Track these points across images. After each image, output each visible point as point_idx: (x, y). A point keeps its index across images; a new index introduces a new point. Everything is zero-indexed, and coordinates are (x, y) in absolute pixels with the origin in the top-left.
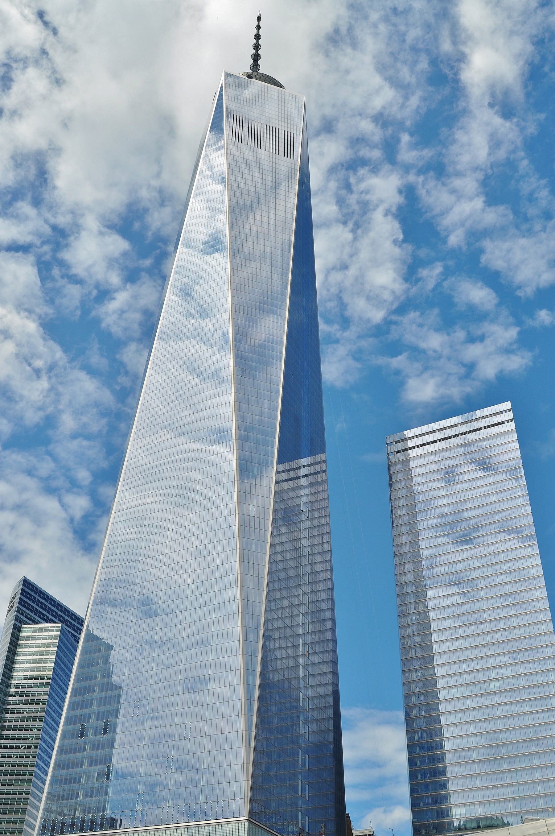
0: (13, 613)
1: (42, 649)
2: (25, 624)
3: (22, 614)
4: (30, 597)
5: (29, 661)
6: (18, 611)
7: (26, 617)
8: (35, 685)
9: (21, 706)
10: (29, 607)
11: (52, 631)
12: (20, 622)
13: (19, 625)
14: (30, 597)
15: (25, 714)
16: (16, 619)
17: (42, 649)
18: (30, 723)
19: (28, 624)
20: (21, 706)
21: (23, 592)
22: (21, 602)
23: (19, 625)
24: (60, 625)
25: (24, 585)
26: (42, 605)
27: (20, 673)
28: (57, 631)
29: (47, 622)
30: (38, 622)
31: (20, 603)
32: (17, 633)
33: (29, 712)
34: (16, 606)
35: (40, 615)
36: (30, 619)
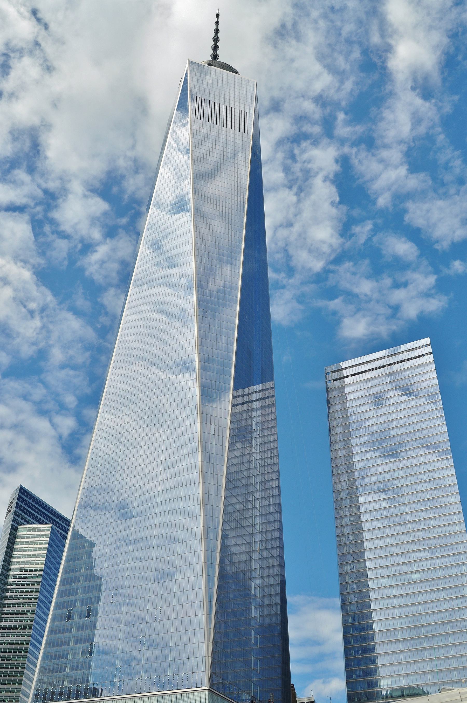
0: (11, 516)
1: (35, 546)
2: (21, 525)
3: (19, 516)
4: (25, 502)
5: (24, 556)
6: (15, 513)
7: (22, 519)
8: (30, 576)
9: (18, 594)
10: (24, 510)
11: (43, 530)
12: (17, 523)
13: (16, 525)
14: (25, 502)
15: (21, 601)
16: (14, 521)
17: (35, 546)
18: (25, 608)
19: (24, 524)
20: (18, 594)
21: (19, 498)
22: (17, 506)
23: (16, 525)
24: (50, 525)
25: (20, 492)
26: (35, 509)
27: (17, 566)
28: (48, 530)
29: (40, 523)
30: (32, 523)
31: (17, 507)
32: (14, 532)
33: (25, 599)
34: (13, 509)
35: (34, 517)
36: (25, 521)
